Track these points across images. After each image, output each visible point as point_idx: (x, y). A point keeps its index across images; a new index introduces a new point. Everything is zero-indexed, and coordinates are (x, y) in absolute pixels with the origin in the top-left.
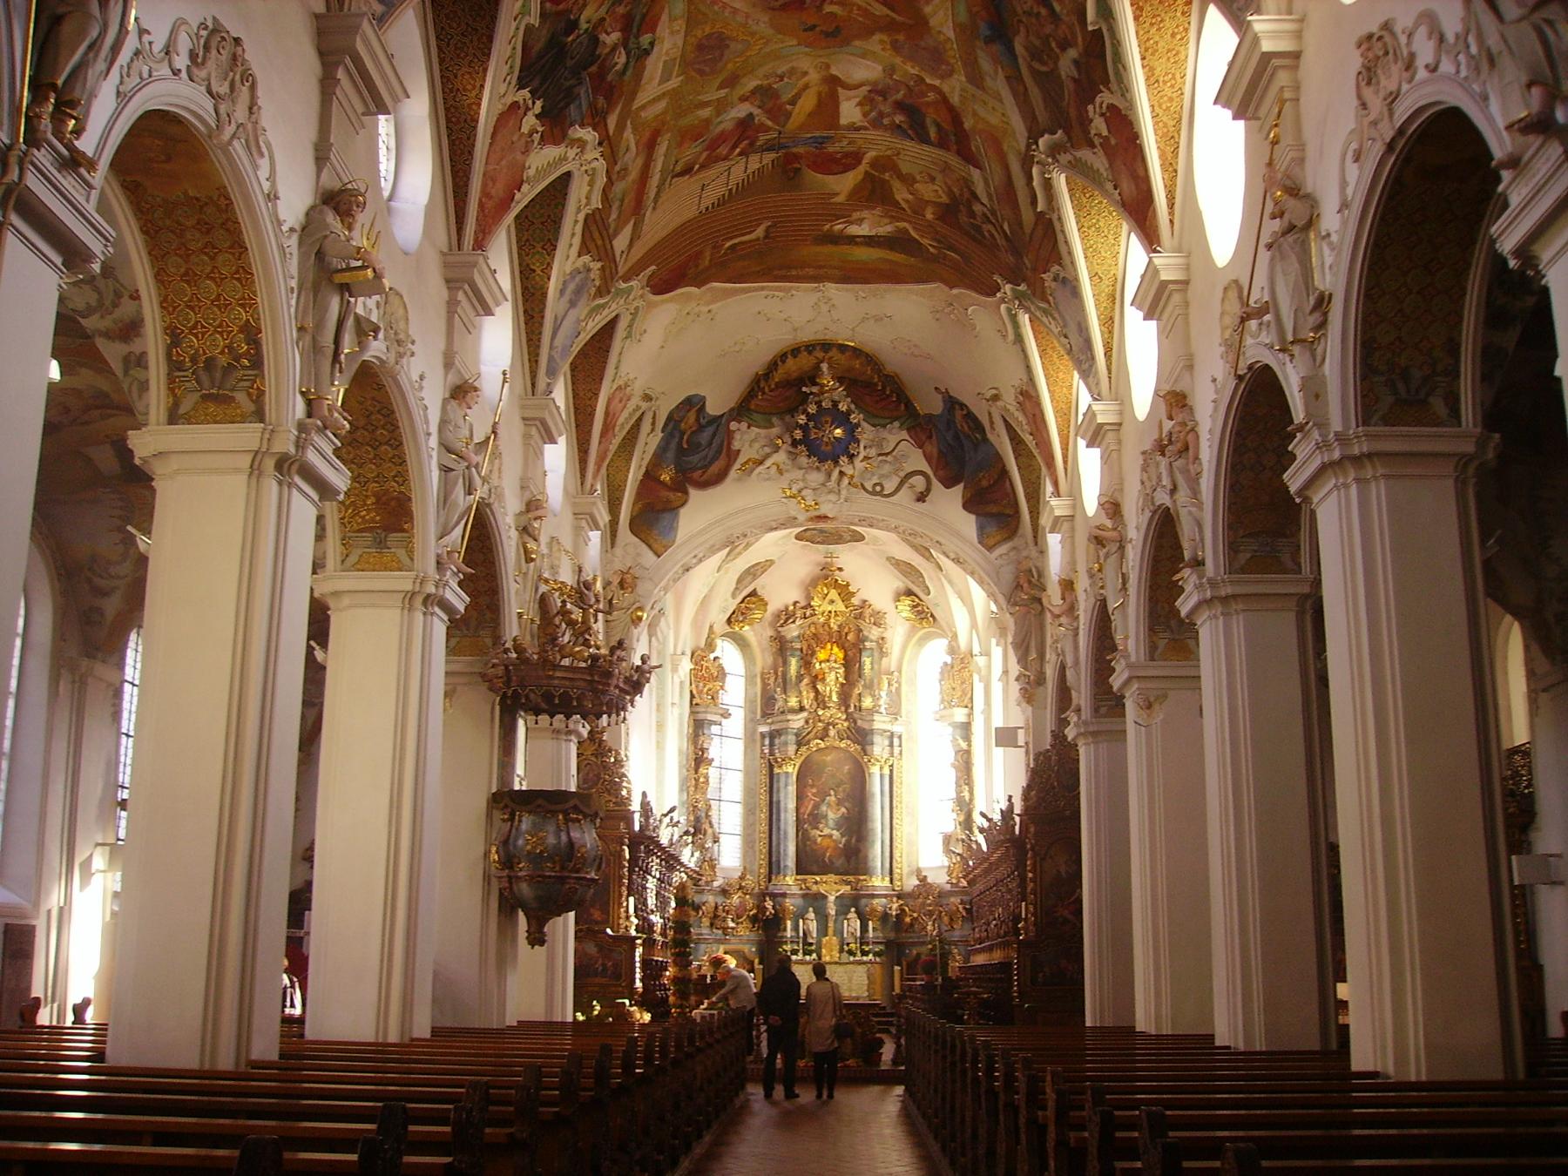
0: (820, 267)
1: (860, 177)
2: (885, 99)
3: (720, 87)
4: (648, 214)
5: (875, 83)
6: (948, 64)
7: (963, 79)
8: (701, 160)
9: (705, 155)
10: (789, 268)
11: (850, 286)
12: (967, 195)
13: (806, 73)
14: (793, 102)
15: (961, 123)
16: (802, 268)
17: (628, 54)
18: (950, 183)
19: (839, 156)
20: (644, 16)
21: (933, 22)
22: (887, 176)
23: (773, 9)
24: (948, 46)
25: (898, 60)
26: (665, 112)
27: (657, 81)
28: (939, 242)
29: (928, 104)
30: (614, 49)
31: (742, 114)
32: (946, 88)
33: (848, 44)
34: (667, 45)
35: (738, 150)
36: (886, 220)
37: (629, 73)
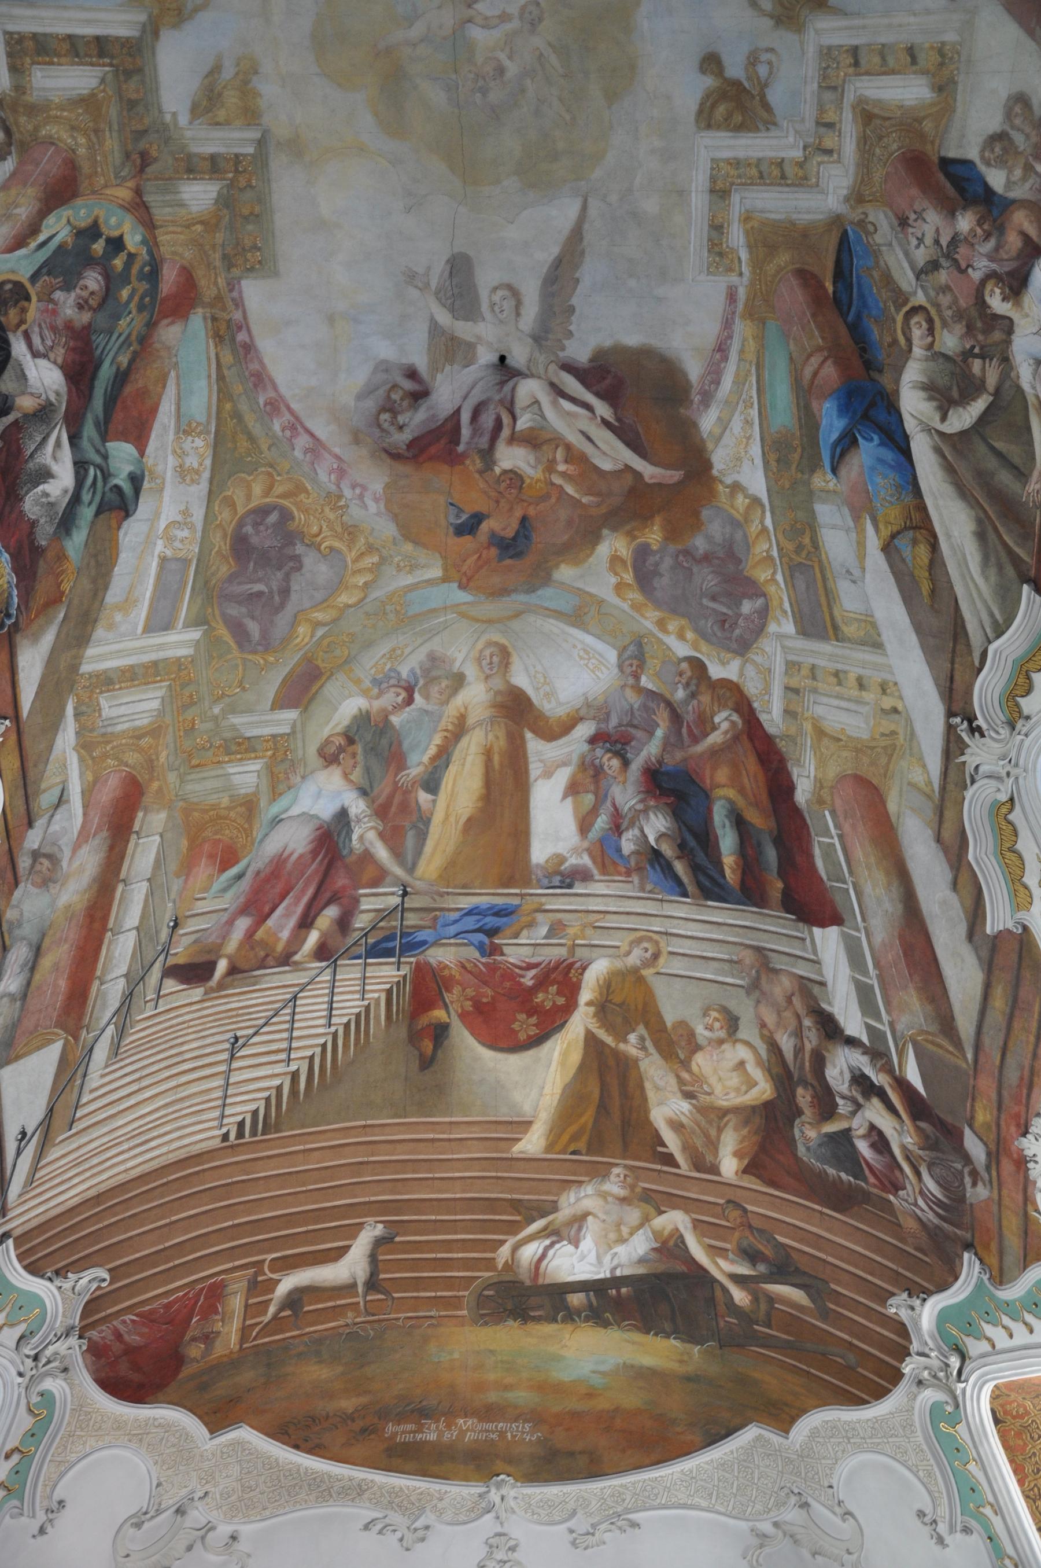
0: (489, 1413)
1: (576, 1057)
2: (626, 763)
3: (280, 703)
4: (101, 1053)
5: (600, 711)
6: (753, 589)
7: (789, 627)
8: (232, 946)
9: (243, 924)
10: (422, 1413)
11: (554, 1491)
12: (812, 1039)
13: (459, 681)
14: (432, 785)
15: (791, 788)
16: (450, 1414)
17: (80, 466)
18: (770, 1019)
19: (528, 979)
20: (122, 378)
21: (719, 459)
22: (631, 1046)
23: (395, 456)
24: (754, 528)
25: (648, 621)
26: (155, 731)
27: (141, 613)
28: (752, 1256)
29: (714, 753)
30: (44, 413)
31: (326, 810)
32: (752, 688)
33: (546, 580)
34: (169, 512)
35: (313, 938)
36: (633, 1215)
37: (79, 537)
